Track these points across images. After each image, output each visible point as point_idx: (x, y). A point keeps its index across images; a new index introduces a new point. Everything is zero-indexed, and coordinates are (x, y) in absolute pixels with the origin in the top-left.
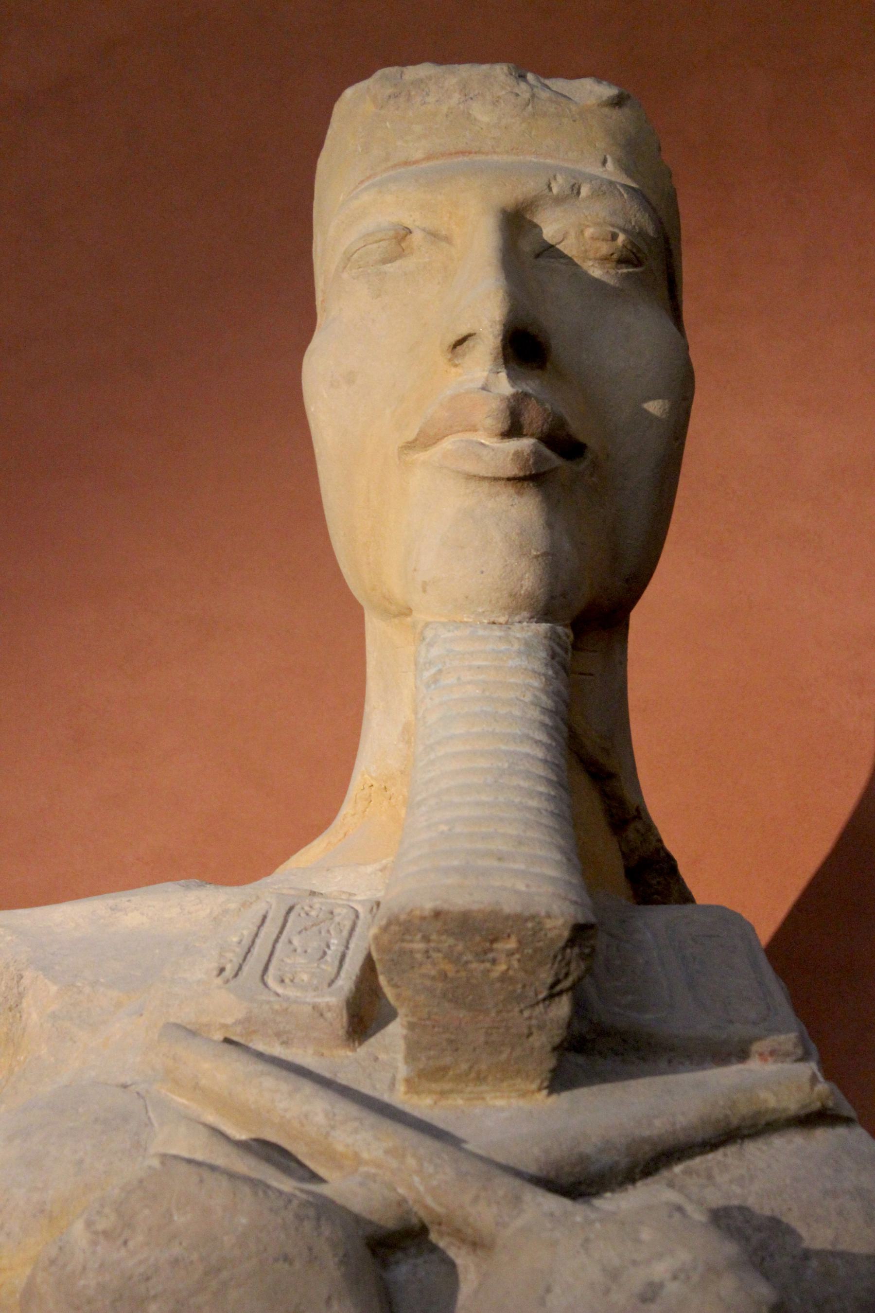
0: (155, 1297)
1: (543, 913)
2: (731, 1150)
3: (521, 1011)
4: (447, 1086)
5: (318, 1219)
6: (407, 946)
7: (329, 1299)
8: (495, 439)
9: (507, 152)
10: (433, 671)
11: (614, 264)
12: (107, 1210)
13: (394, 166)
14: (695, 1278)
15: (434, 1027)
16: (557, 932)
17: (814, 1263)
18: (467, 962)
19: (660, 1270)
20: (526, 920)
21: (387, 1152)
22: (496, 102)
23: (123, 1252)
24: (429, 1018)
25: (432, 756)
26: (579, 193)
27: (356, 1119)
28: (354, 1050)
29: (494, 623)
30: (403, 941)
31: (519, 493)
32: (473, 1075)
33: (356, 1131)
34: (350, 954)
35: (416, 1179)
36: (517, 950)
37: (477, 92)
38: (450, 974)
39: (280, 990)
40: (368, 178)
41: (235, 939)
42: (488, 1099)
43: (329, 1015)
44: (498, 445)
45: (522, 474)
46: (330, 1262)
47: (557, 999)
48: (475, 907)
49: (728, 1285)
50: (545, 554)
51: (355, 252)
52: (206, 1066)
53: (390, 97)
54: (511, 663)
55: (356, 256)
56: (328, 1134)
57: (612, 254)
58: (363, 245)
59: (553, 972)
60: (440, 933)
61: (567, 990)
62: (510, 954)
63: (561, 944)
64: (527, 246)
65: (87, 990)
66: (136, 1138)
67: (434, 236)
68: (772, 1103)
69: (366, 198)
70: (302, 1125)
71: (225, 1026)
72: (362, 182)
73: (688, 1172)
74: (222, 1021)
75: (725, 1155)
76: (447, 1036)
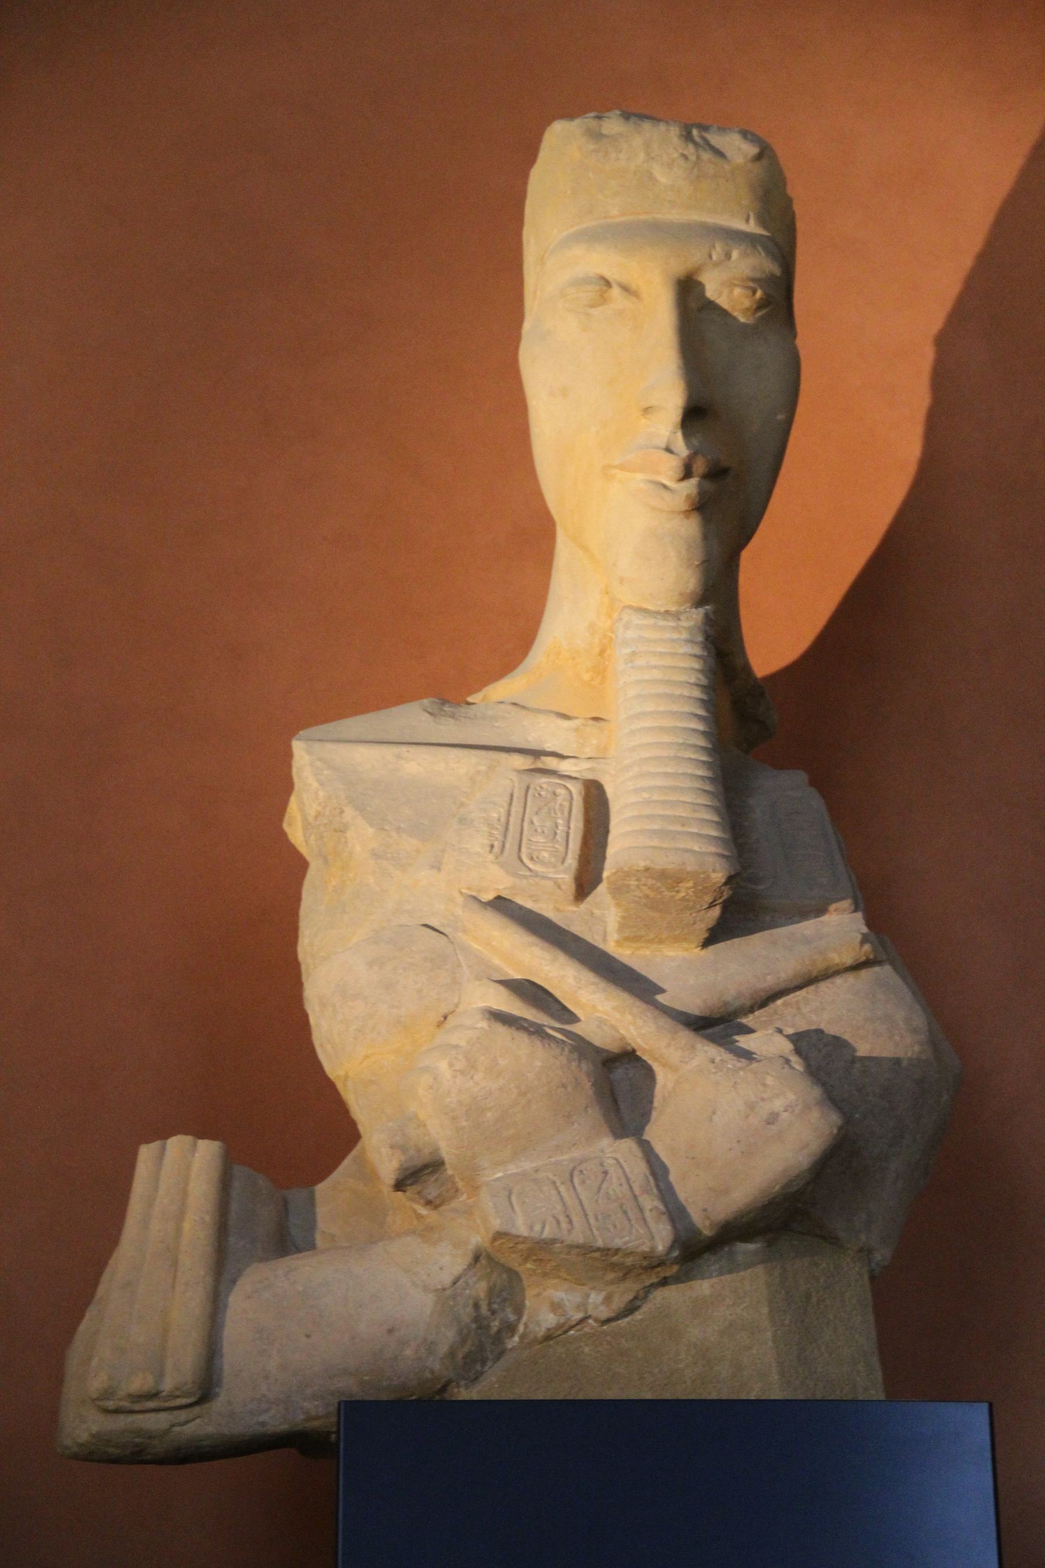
2: (811, 988)
5: (580, 1060)
6: (627, 882)
7: (586, 1107)
12: (460, 1057)
14: (797, 1112)
16: (718, 879)
17: (858, 1065)
19: (778, 1104)
21: (614, 1008)
22: (670, 165)
23: (471, 1083)
27: (593, 984)
28: (578, 907)
30: (624, 880)
32: (657, 940)
34: (572, 831)
35: (632, 1028)
36: (693, 887)
39: (531, 866)
41: (496, 815)
43: (563, 887)
46: (588, 1085)
47: (713, 908)
49: (815, 1114)
50: (704, 562)
52: (496, 933)
54: (681, 650)
61: (720, 904)
62: (689, 888)
64: (693, 305)
65: (394, 834)
67: (626, 289)
71: (498, 890)
73: (785, 1005)
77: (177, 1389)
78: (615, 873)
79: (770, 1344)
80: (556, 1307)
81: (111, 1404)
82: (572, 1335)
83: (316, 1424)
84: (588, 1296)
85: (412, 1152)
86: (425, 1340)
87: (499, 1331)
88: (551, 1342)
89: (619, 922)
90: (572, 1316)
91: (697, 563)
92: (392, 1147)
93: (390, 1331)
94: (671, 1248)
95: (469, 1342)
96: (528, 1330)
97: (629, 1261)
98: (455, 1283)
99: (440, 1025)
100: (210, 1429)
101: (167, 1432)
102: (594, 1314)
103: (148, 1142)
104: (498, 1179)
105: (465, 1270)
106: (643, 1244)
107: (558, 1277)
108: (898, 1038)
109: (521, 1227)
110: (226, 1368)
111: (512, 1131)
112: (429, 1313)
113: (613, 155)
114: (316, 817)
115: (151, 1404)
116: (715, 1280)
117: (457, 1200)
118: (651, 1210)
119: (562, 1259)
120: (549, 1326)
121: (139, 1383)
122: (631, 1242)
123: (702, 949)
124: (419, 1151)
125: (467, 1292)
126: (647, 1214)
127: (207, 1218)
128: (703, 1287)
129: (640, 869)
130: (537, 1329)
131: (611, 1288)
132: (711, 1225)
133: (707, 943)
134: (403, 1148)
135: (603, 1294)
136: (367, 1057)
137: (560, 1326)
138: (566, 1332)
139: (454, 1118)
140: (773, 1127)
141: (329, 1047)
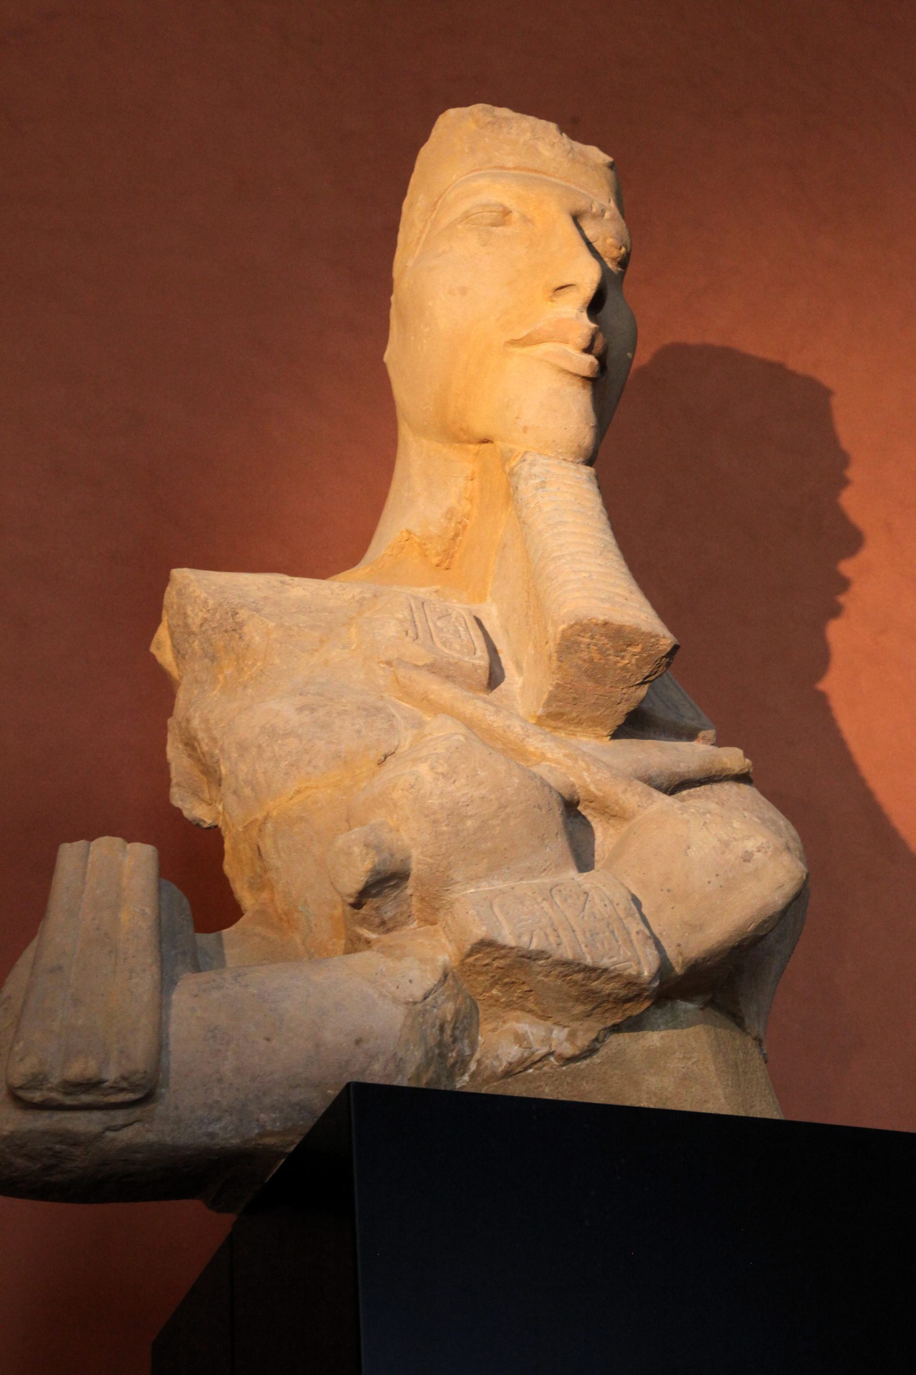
0: (471, 816)
1: (662, 635)
2: (708, 787)
3: (623, 689)
4: (560, 724)
6: (580, 639)
7: (557, 833)
8: (578, 352)
9: (560, 178)
10: (538, 481)
11: (616, 263)
12: (441, 761)
13: (494, 167)
14: (769, 853)
15: (570, 689)
16: (665, 647)
18: (609, 655)
19: (750, 845)
20: (652, 637)
21: (566, 756)
22: (553, 145)
23: (453, 787)
24: (570, 684)
25: (555, 531)
26: (603, 216)
28: (488, 694)
29: (565, 460)
30: (579, 635)
31: (584, 387)
33: (543, 741)
35: (585, 774)
37: (540, 136)
38: (595, 660)
40: (477, 170)
42: (578, 736)
43: (479, 671)
44: (579, 355)
45: (591, 376)
48: (627, 624)
51: (474, 214)
53: (489, 123)
55: (473, 217)
57: (618, 258)
58: (482, 211)
59: (651, 670)
60: (602, 635)
63: (663, 655)
66: (390, 723)
68: (729, 766)
69: (483, 182)
70: (505, 732)
72: (473, 171)
74: (416, 663)
75: (705, 790)
76: (574, 695)
77: (124, 1078)
78: (571, 627)
79: (723, 1100)
80: (520, 1039)
81: (37, 1096)
82: (530, 1074)
83: (270, 1141)
84: (551, 1031)
85: (385, 855)
86: (395, 1054)
87: (453, 1066)
88: (510, 1080)
89: (551, 692)
90: (537, 1050)
91: (592, 425)
92: (367, 846)
93: (358, 1042)
94: (653, 979)
95: (432, 1068)
96: (482, 1067)
97: (608, 988)
98: (425, 998)
99: (380, 763)
100: (151, 1137)
101: (99, 1136)
102: (559, 1050)
103: (71, 841)
104: (471, 893)
105: (435, 985)
106: (631, 967)
107: (523, 1009)
109: (507, 937)
110: (174, 1066)
111: (489, 845)
112: (399, 1026)
113: (506, 130)
114: (201, 625)
115: (86, 1098)
116: (663, 1033)
117: (408, 928)
118: (638, 933)
119: (539, 981)
120: (509, 1060)
121: (76, 1070)
122: (619, 963)
123: (611, 739)
124: (392, 855)
125: (435, 1010)
126: (634, 936)
128: (653, 1038)
129: (599, 622)
130: (496, 1063)
131: (575, 1025)
132: (683, 962)
133: (615, 736)
134: (378, 849)
135: (566, 1030)
136: (298, 792)
137: (521, 1061)
138: (526, 1069)
139: (435, 822)
140: (750, 865)
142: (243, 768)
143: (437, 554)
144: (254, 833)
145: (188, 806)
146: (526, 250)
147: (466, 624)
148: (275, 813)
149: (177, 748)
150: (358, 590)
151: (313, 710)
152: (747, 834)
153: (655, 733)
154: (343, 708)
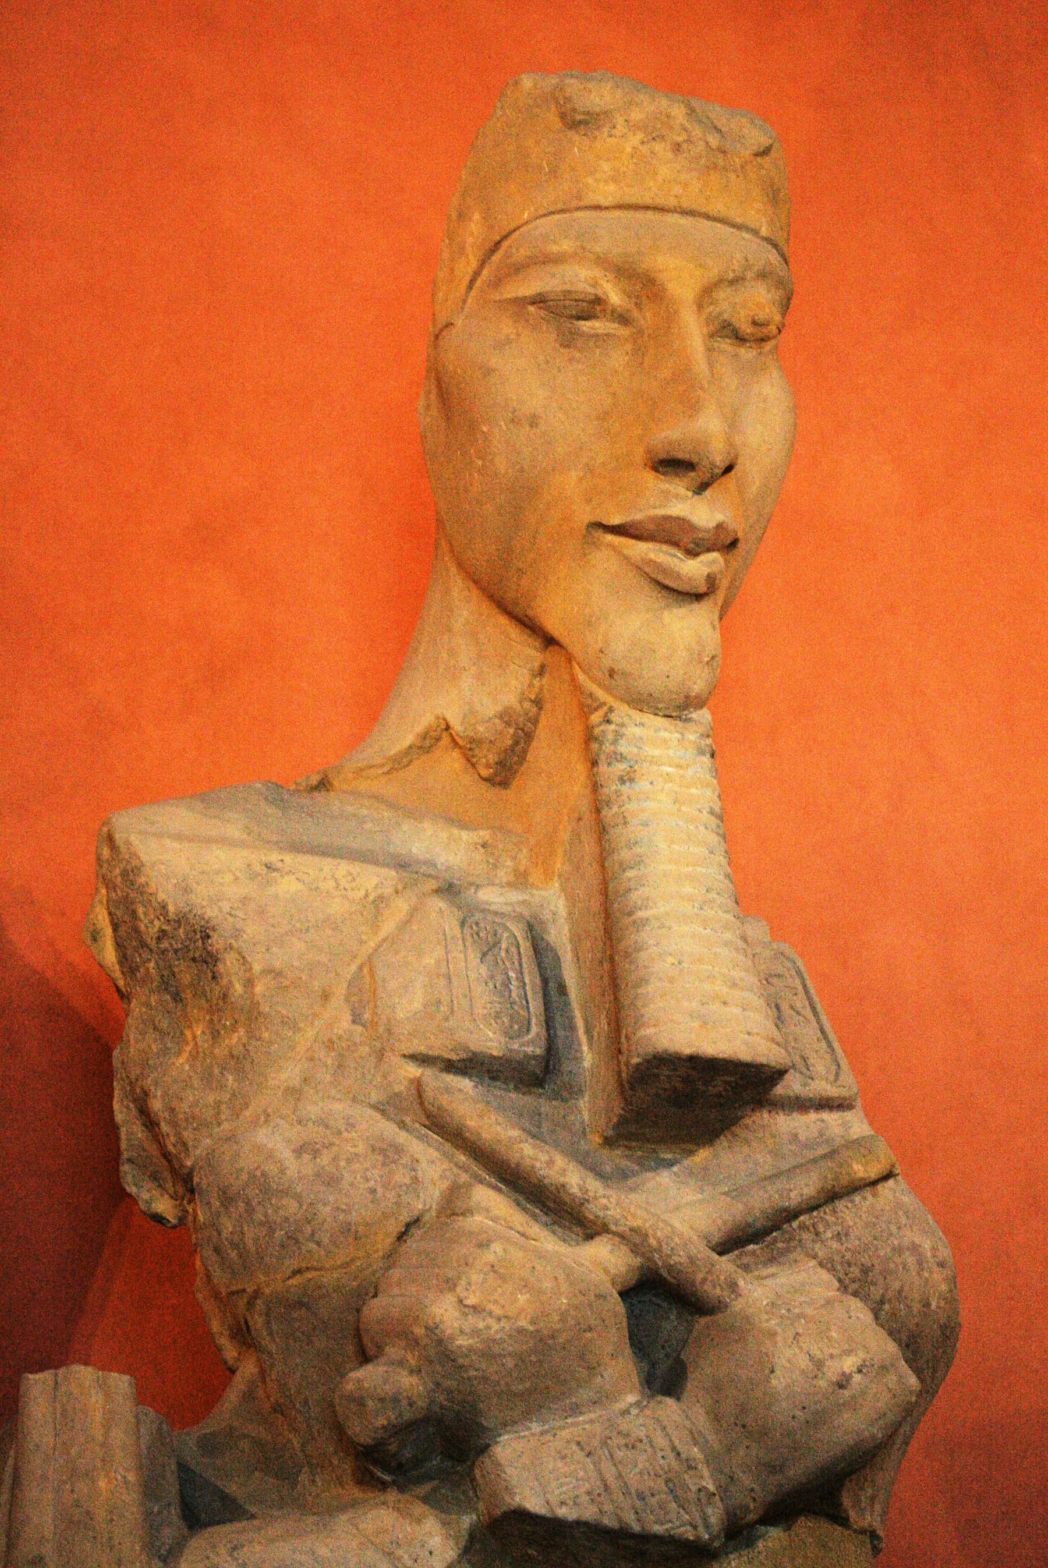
17: (887, 1307)
55: (551, 303)
56: (582, 1204)
68: (861, 1174)
73: (803, 1227)
108: (926, 1274)
114: (159, 939)
127: (131, 1477)
136: (298, 1272)
140: (845, 1392)
141: (233, 1254)
142: (228, 1226)
143: (488, 766)
144: (242, 1303)
145: (145, 1196)
146: (627, 358)
147: (521, 965)
148: (267, 1291)
149: (127, 1107)
150: (375, 881)
151: (316, 1154)
152: (846, 1347)
153: (770, 1112)
154: (352, 1150)
